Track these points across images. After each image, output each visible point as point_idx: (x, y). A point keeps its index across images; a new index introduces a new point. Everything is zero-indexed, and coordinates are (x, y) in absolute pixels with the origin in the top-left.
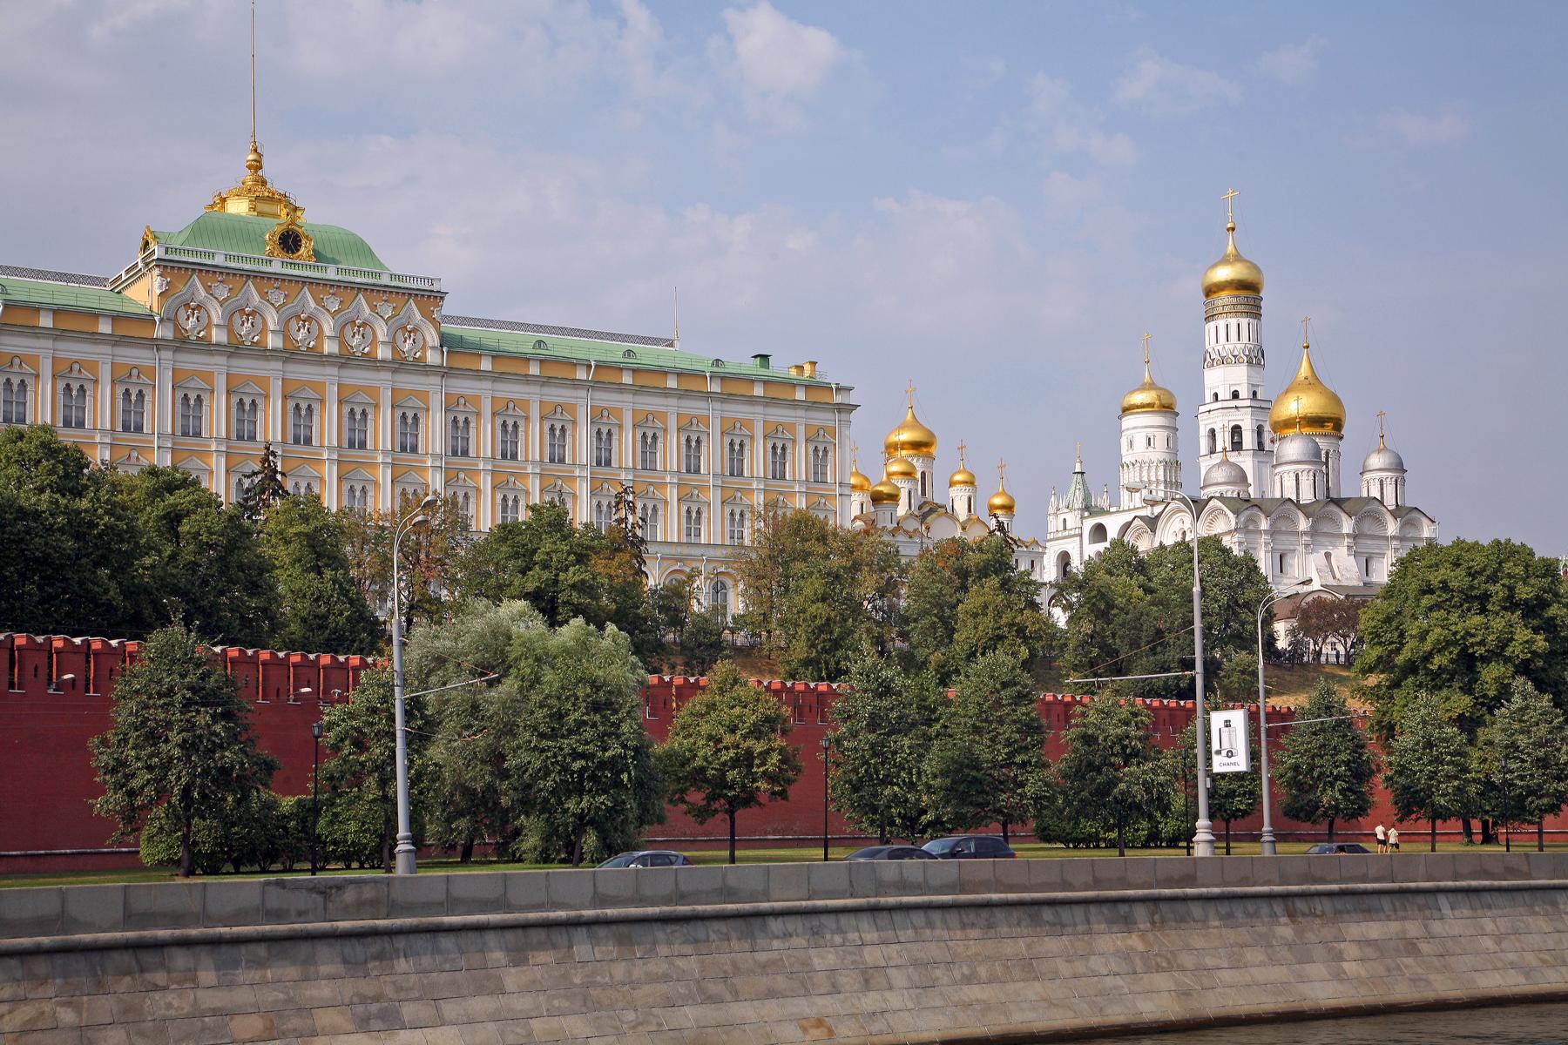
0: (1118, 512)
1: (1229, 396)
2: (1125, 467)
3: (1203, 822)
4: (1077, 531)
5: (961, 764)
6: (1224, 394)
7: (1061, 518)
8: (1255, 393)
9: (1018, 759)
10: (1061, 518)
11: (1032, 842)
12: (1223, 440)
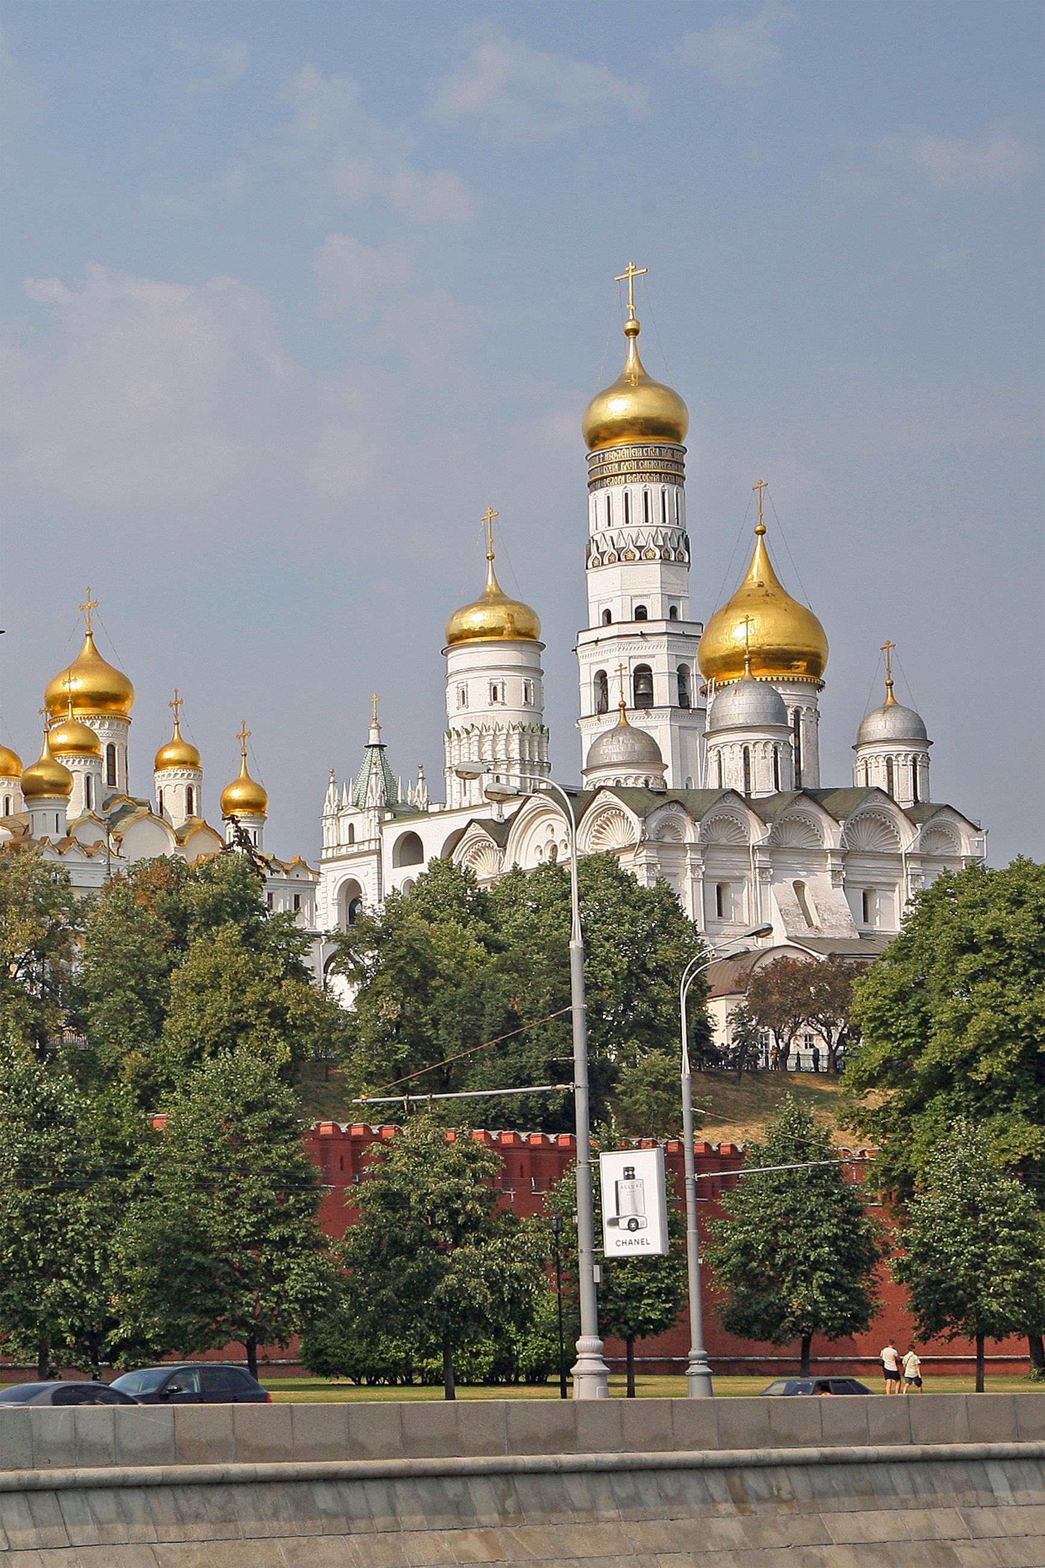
0: (441, 812)
1: (630, 616)
2: (454, 737)
3: (588, 1341)
4: (373, 846)
5: (177, 1242)
6: (622, 612)
7: (345, 823)
8: (673, 611)
9: (274, 1234)
10: (345, 823)
11: (298, 1376)
12: (621, 691)
